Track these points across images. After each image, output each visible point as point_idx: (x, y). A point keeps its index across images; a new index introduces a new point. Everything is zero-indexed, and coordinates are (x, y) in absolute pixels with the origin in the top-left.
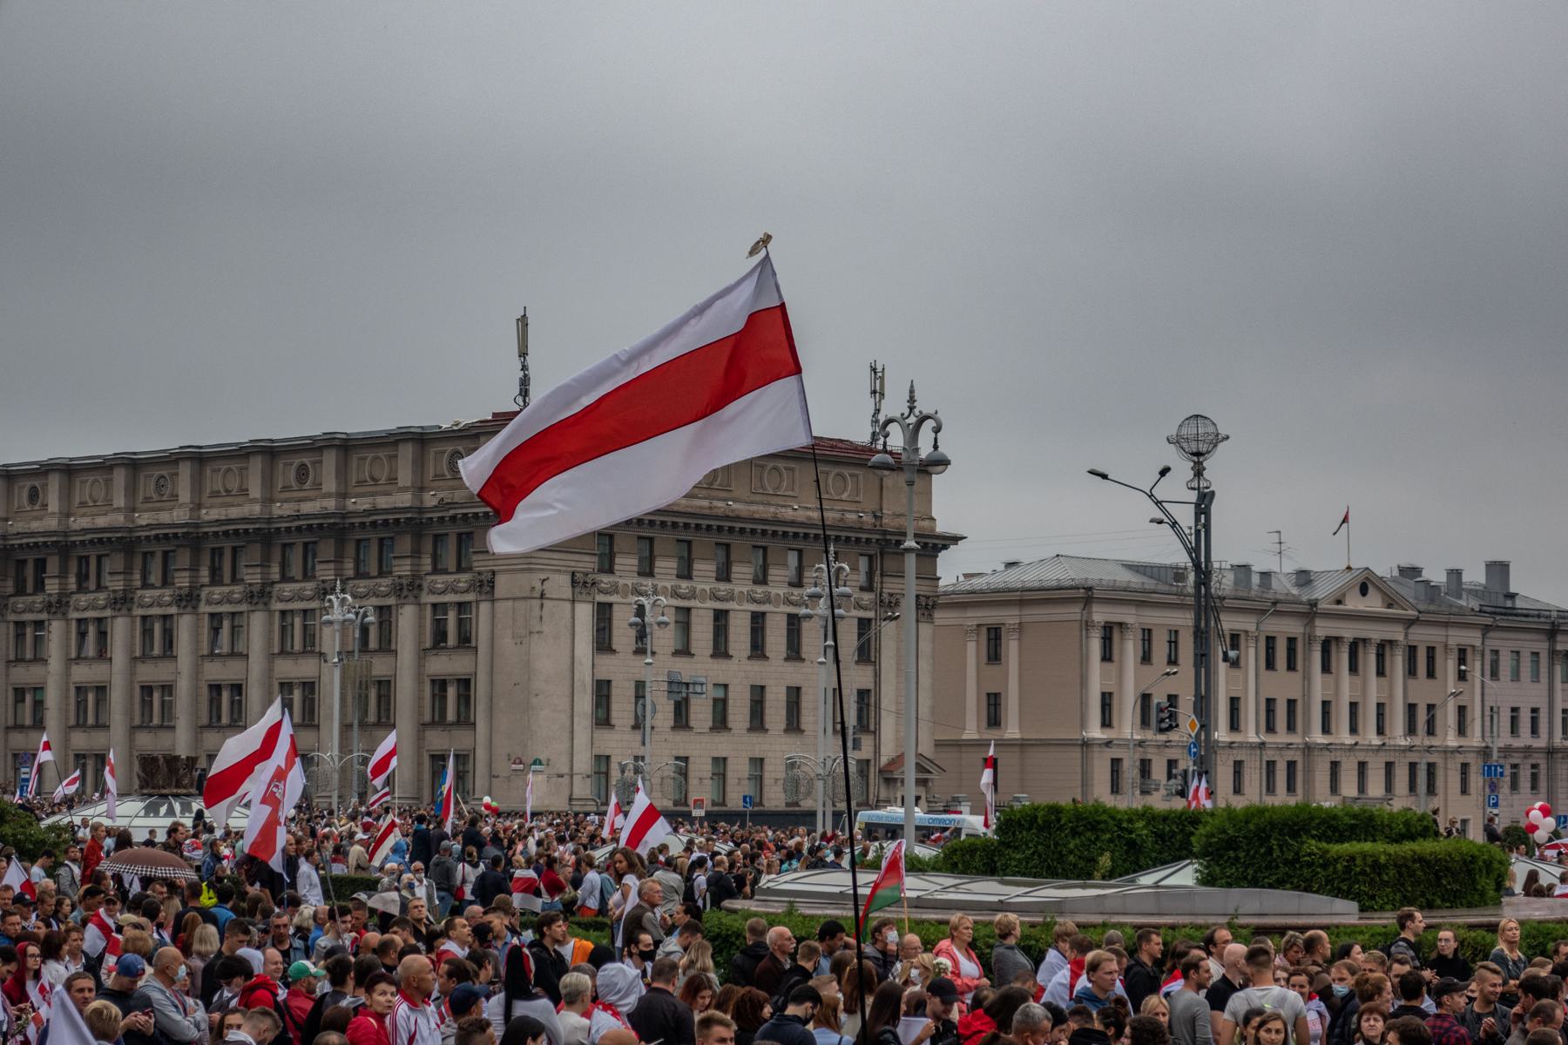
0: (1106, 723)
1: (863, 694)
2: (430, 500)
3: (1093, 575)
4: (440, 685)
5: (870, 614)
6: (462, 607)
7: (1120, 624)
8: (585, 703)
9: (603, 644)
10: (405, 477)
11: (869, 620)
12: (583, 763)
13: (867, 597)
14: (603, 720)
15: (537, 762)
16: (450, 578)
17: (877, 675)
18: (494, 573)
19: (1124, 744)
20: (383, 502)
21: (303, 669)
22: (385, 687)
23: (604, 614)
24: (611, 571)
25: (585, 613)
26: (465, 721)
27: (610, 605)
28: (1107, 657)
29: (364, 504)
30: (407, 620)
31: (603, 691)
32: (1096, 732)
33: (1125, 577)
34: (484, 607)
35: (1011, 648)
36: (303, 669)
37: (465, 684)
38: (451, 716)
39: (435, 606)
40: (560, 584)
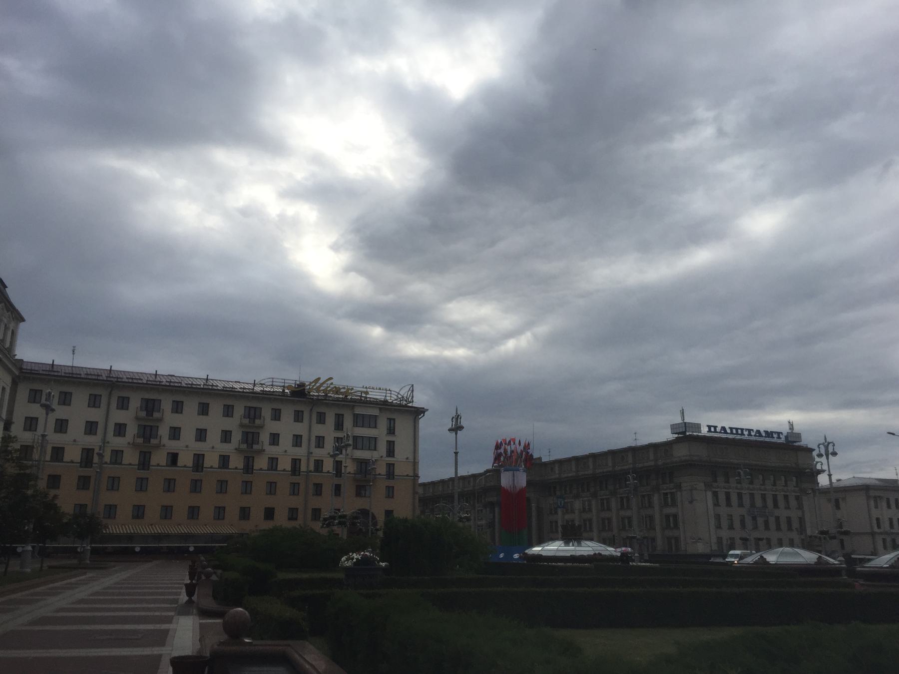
0: (879, 527)
1: (800, 519)
2: (660, 463)
3: (868, 482)
4: (667, 517)
5: (799, 494)
6: (672, 493)
7: (879, 497)
8: (713, 522)
9: (716, 504)
10: (652, 457)
11: (798, 496)
12: (714, 540)
13: (797, 489)
14: (719, 527)
15: (700, 539)
16: (668, 485)
17: (803, 512)
18: (681, 483)
19: (886, 533)
20: (646, 464)
21: (628, 513)
22: (651, 518)
23: (715, 494)
24: (716, 481)
25: (709, 494)
26: (676, 526)
27: (717, 492)
28: (876, 507)
29: (641, 465)
30: (656, 499)
31: (718, 517)
32: (876, 529)
33: (877, 482)
34: (679, 493)
35: (842, 504)
36: (628, 513)
37: (675, 516)
38: (672, 525)
39: (664, 493)
40: (701, 486)
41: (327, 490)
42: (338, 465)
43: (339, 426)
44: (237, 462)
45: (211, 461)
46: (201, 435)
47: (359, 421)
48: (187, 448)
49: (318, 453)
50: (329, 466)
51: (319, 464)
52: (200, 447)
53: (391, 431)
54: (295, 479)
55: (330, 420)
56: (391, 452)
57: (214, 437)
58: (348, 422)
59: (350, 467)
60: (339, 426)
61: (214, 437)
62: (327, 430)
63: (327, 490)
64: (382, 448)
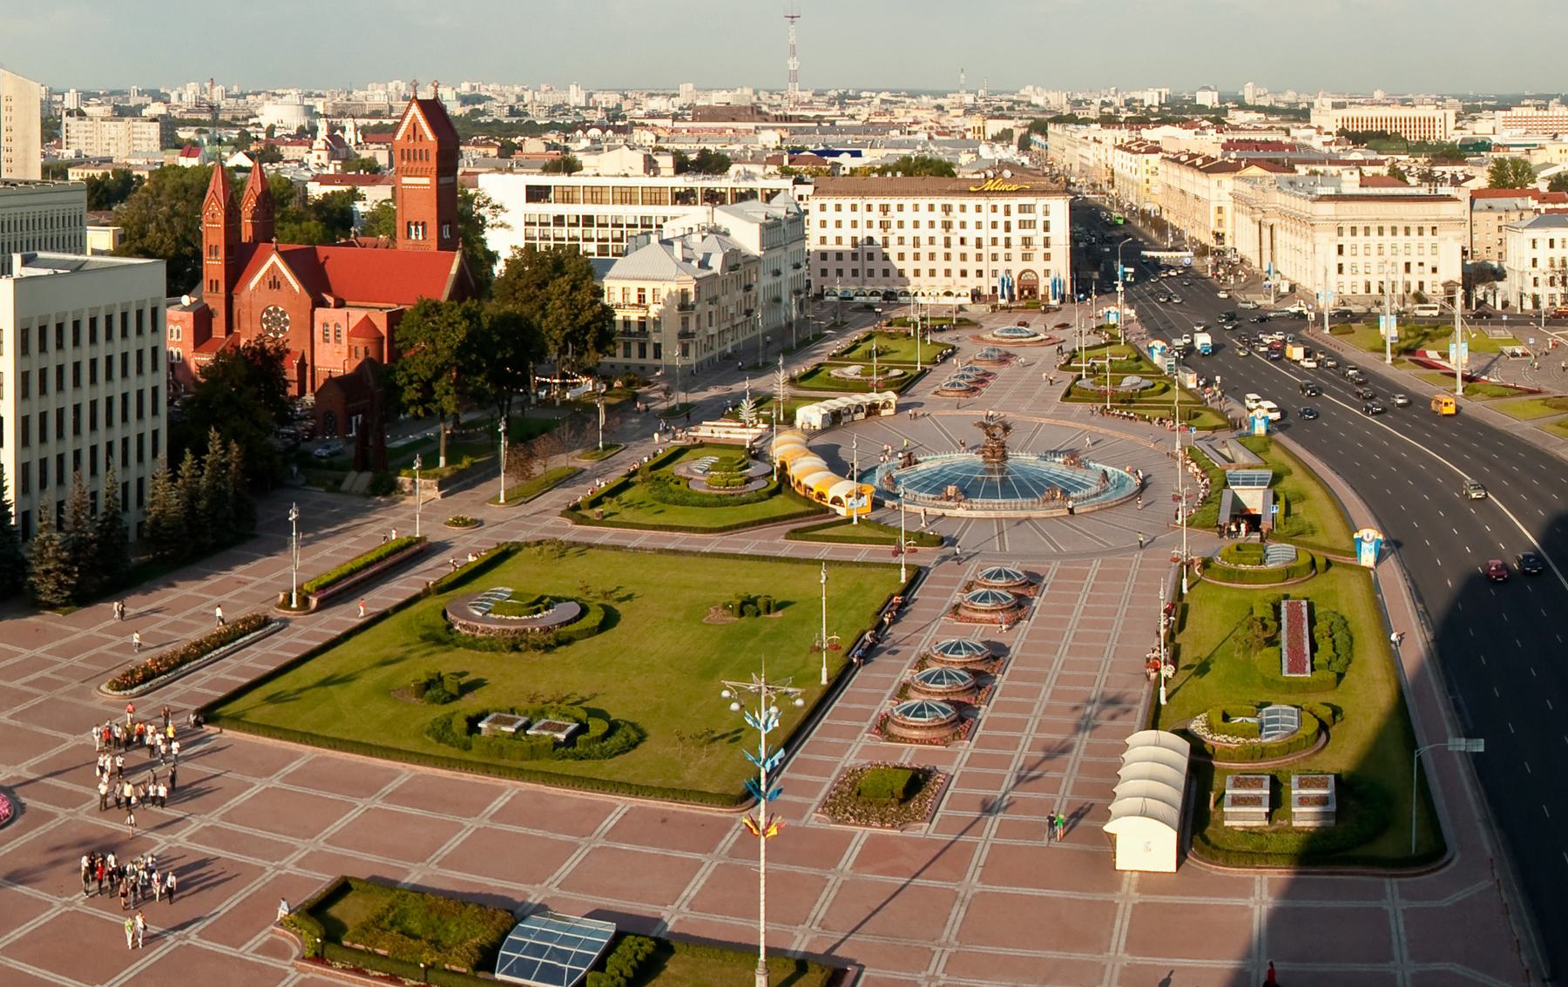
41: (1001, 257)
42: (1008, 241)
43: (1008, 213)
44: (940, 241)
45: (924, 241)
46: (916, 225)
47: (1023, 209)
48: (908, 233)
49: (994, 233)
50: (1001, 242)
51: (994, 241)
52: (916, 233)
53: (1046, 213)
54: (979, 251)
55: (1001, 209)
56: (1046, 229)
57: (924, 225)
58: (1014, 210)
59: (1016, 240)
60: (1008, 213)
61: (924, 225)
62: (1000, 218)
63: (1001, 257)
64: (1040, 225)
